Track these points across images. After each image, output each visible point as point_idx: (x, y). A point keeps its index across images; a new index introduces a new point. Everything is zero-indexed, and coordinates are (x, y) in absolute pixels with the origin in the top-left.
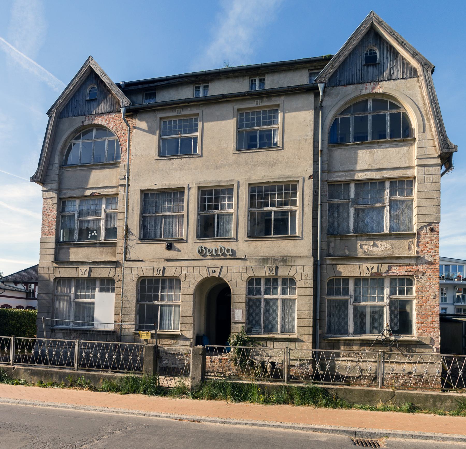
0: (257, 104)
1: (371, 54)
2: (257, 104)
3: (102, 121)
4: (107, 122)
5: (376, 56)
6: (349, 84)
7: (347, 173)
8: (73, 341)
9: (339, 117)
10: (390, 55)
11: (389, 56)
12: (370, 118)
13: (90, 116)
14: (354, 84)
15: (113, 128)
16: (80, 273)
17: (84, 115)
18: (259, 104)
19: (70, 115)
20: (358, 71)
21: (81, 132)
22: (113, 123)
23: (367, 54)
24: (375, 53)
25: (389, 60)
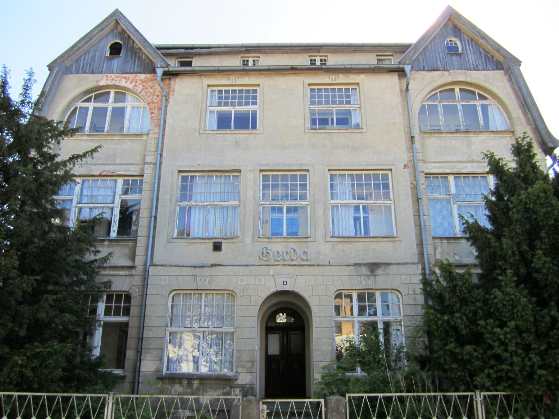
0: (332, 80)
1: (451, 44)
2: (332, 80)
3: (126, 82)
4: (134, 84)
5: (458, 47)
6: (434, 70)
7: (444, 165)
8: (102, 395)
9: (426, 104)
10: (472, 47)
11: (471, 48)
12: (460, 107)
13: (109, 75)
14: (440, 70)
15: (140, 92)
16: (199, 283)
17: (101, 73)
18: (335, 80)
19: (80, 71)
20: (441, 59)
21: (93, 94)
22: (141, 86)
23: (447, 44)
24: (456, 44)
25: (472, 51)
